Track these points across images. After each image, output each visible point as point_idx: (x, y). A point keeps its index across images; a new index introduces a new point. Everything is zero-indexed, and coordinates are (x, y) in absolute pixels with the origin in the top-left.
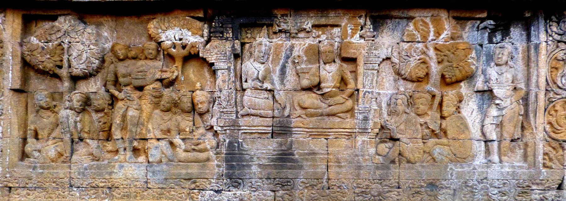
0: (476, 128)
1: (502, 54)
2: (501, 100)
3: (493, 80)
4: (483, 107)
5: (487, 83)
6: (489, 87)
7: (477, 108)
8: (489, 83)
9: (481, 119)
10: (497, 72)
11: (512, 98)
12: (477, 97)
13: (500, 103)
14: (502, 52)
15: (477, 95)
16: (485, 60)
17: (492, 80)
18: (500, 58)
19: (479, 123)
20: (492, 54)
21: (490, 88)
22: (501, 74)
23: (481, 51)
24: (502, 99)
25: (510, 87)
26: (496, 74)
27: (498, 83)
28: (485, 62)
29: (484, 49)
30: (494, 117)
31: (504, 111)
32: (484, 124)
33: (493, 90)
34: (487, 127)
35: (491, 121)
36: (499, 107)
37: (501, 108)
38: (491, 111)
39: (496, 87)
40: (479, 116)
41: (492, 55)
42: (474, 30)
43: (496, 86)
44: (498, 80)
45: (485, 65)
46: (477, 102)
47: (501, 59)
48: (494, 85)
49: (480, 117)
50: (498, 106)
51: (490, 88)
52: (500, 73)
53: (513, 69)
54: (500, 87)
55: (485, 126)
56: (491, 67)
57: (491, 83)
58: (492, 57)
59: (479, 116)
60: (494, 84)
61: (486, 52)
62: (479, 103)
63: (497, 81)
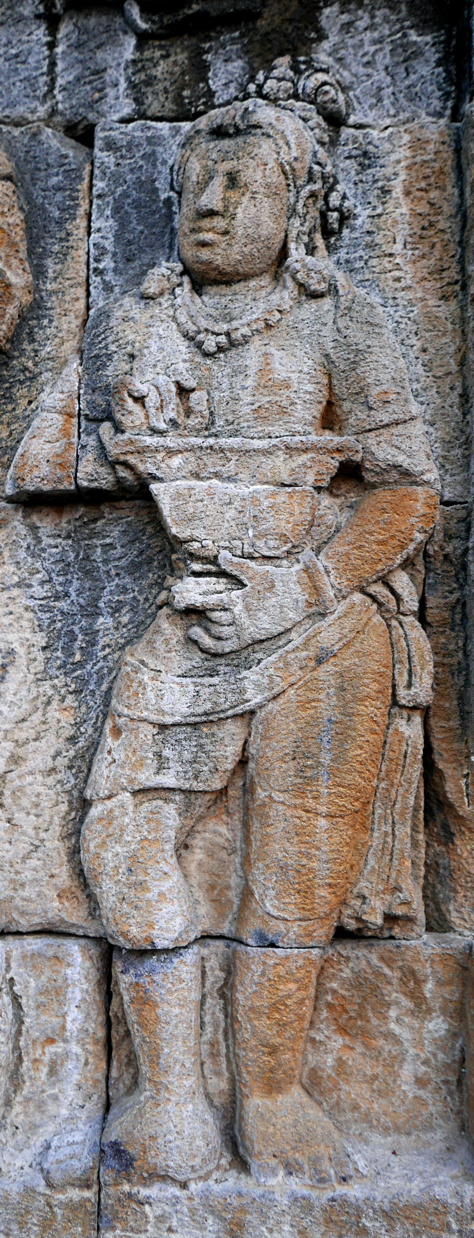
0: (28, 823)
1: (232, 180)
2: (222, 574)
3: (152, 400)
4: (92, 635)
5: (106, 428)
6: (113, 464)
7: (41, 639)
8: (118, 429)
9: (72, 740)
10: (188, 337)
11: (322, 562)
12: (35, 551)
13: (213, 599)
14: (226, 166)
15: (34, 529)
16: (109, 244)
17: (140, 400)
18: (212, 213)
19: (53, 770)
20: (163, 196)
21: (126, 465)
22: (220, 349)
23: (74, 176)
24: (229, 569)
25: (304, 458)
26: (183, 346)
27: (193, 421)
28: (107, 263)
29: (101, 155)
30: (163, 727)
31: (252, 675)
32: (88, 794)
33: (155, 487)
34: (108, 818)
35: (141, 763)
36: (207, 642)
37: (228, 646)
38: (146, 677)
39: (176, 461)
40: (53, 712)
41: (168, 202)
42: (21, 19)
43: (171, 452)
44: (198, 398)
45: (108, 288)
46: (39, 591)
47: (219, 223)
48: (151, 441)
49: (67, 719)
50: (197, 632)
51: (123, 473)
52: (210, 344)
53: (327, 303)
54: (212, 463)
55: (95, 812)
56: (146, 298)
57: (127, 421)
58: (170, 216)
59: (53, 712)
60: (155, 431)
61: (116, 179)
62: (57, 598)
63: (188, 412)
